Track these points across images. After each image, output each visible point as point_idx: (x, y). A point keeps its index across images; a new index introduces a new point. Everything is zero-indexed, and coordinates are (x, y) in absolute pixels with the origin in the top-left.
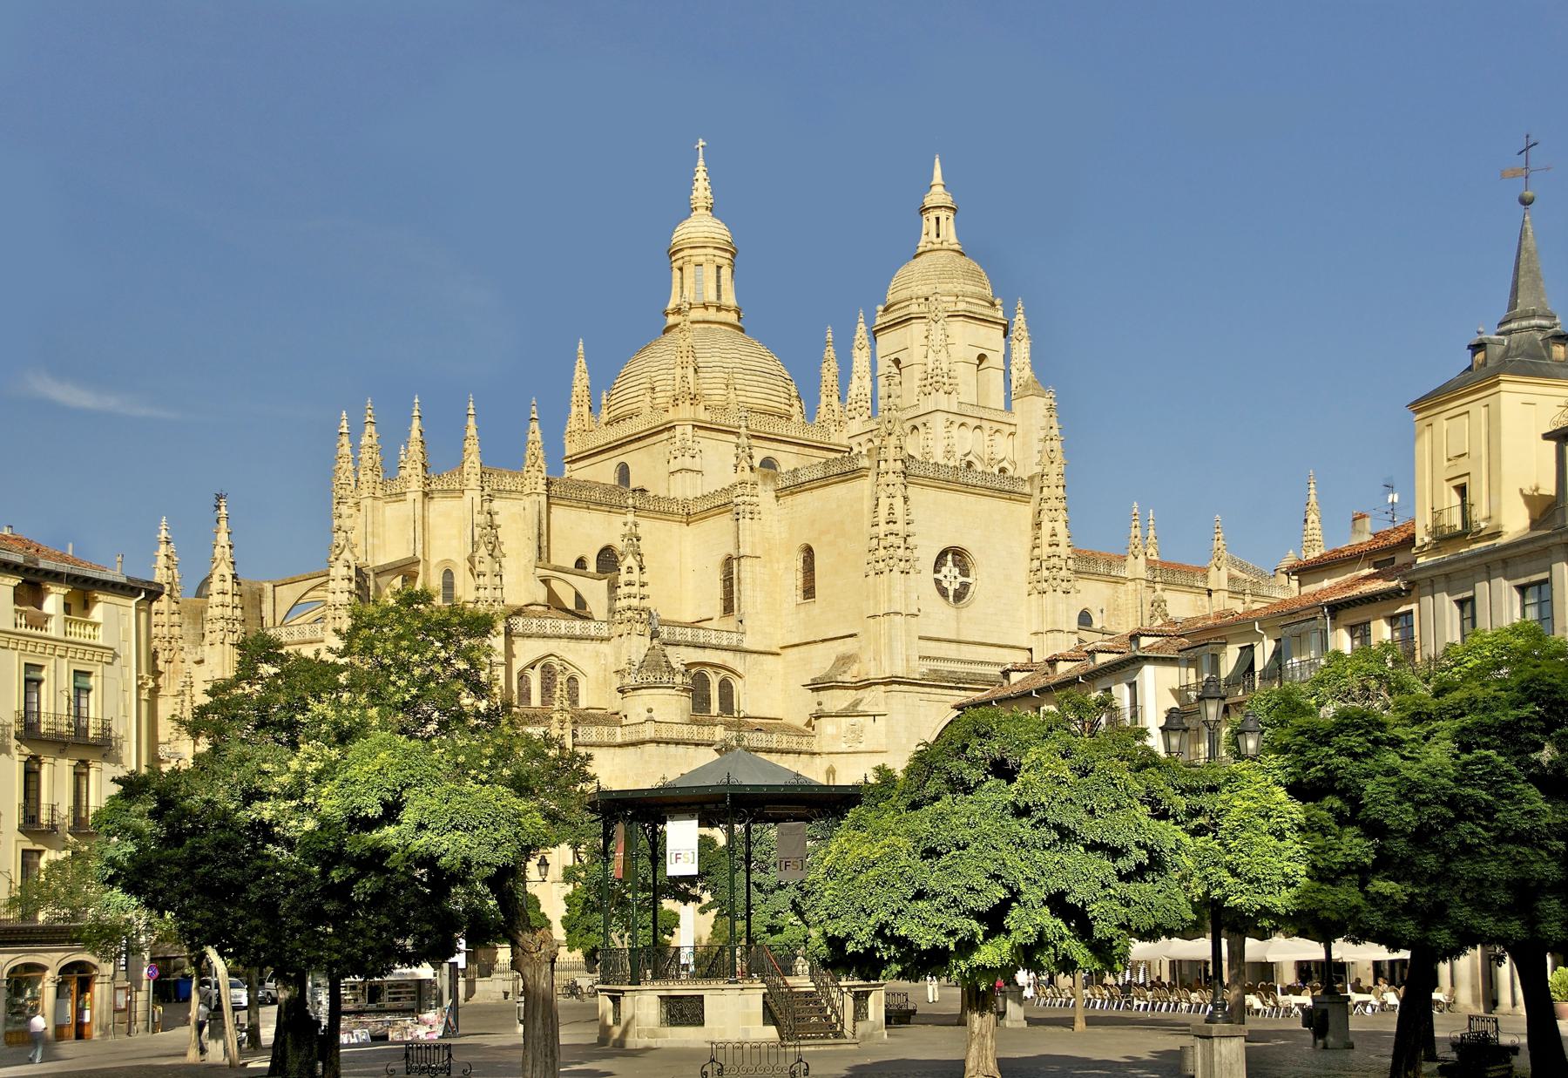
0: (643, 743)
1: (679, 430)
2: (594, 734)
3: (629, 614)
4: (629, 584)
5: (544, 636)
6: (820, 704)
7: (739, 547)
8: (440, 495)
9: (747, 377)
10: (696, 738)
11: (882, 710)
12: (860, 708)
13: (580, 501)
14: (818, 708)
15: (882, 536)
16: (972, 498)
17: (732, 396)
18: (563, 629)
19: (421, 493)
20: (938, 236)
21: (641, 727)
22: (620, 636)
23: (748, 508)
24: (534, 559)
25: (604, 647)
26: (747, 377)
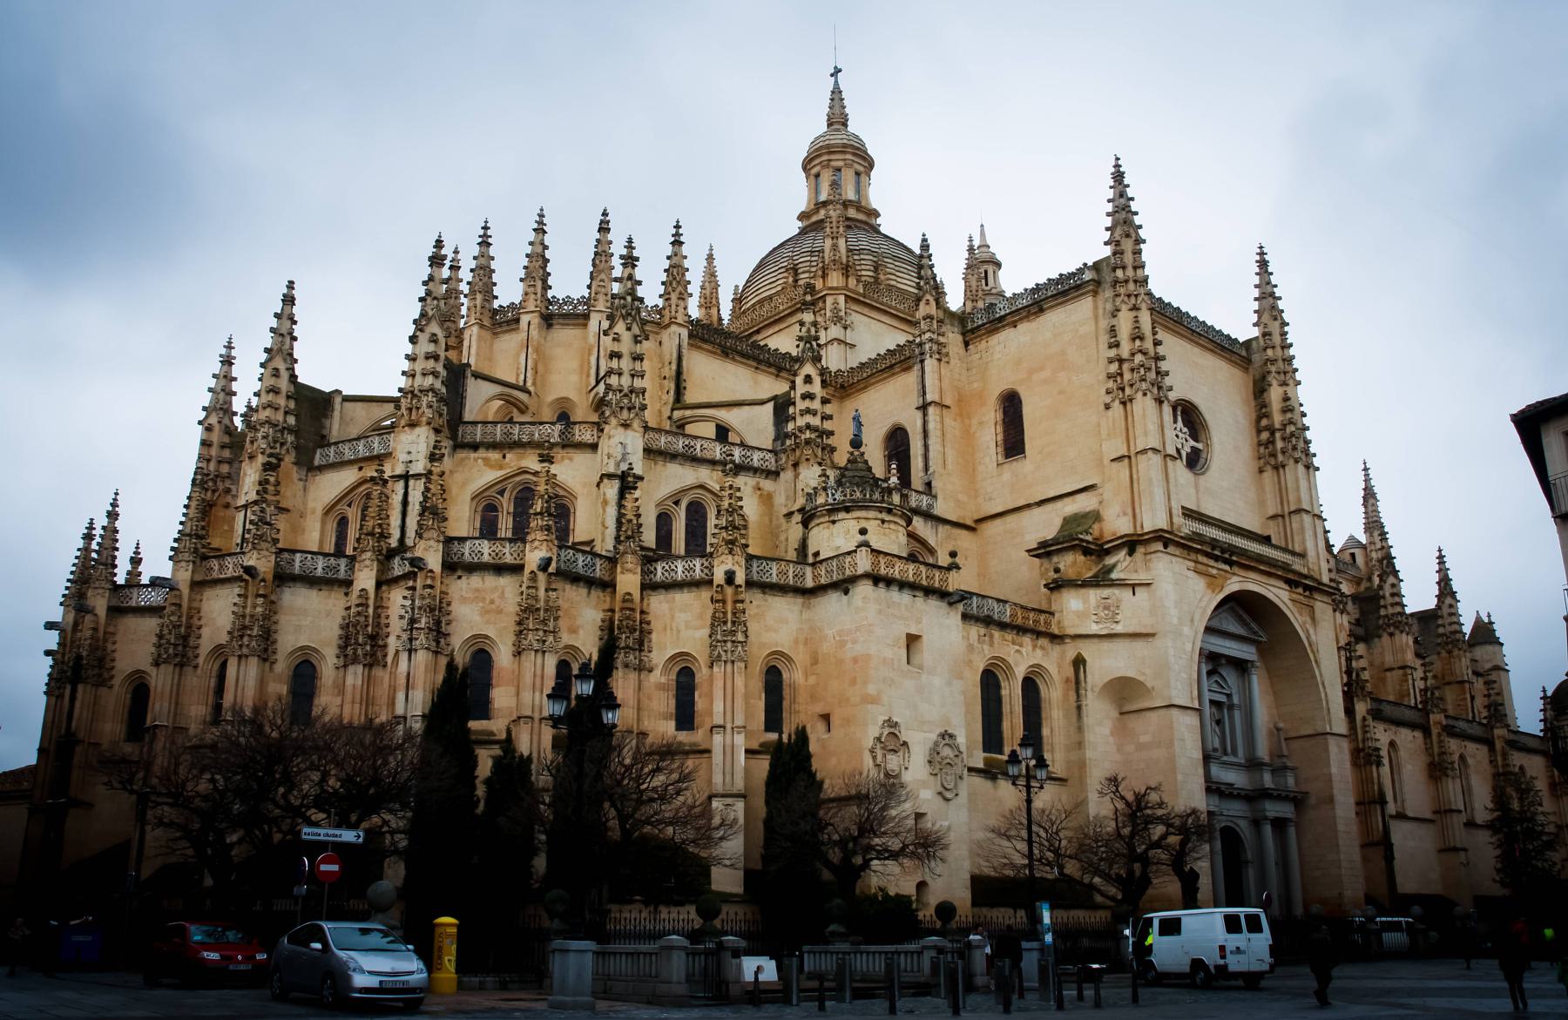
0: (854, 579)
1: (829, 300)
2: (774, 572)
3: (808, 435)
4: (808, 396)
6: (1057, 570)
7: (924, 393)
8: (561, 321)
9: (897, 263)
11: (1142, 576)
12: (1114, 576)
14: (1052, 575)
15: (1125, 354)
16: (1196, 350)
17: (882, 277)
20: (987, 285)
21: (848, 559)
22: (796, 465)
23: (935, 347)
25: (767, 485)
26: (897, 263)
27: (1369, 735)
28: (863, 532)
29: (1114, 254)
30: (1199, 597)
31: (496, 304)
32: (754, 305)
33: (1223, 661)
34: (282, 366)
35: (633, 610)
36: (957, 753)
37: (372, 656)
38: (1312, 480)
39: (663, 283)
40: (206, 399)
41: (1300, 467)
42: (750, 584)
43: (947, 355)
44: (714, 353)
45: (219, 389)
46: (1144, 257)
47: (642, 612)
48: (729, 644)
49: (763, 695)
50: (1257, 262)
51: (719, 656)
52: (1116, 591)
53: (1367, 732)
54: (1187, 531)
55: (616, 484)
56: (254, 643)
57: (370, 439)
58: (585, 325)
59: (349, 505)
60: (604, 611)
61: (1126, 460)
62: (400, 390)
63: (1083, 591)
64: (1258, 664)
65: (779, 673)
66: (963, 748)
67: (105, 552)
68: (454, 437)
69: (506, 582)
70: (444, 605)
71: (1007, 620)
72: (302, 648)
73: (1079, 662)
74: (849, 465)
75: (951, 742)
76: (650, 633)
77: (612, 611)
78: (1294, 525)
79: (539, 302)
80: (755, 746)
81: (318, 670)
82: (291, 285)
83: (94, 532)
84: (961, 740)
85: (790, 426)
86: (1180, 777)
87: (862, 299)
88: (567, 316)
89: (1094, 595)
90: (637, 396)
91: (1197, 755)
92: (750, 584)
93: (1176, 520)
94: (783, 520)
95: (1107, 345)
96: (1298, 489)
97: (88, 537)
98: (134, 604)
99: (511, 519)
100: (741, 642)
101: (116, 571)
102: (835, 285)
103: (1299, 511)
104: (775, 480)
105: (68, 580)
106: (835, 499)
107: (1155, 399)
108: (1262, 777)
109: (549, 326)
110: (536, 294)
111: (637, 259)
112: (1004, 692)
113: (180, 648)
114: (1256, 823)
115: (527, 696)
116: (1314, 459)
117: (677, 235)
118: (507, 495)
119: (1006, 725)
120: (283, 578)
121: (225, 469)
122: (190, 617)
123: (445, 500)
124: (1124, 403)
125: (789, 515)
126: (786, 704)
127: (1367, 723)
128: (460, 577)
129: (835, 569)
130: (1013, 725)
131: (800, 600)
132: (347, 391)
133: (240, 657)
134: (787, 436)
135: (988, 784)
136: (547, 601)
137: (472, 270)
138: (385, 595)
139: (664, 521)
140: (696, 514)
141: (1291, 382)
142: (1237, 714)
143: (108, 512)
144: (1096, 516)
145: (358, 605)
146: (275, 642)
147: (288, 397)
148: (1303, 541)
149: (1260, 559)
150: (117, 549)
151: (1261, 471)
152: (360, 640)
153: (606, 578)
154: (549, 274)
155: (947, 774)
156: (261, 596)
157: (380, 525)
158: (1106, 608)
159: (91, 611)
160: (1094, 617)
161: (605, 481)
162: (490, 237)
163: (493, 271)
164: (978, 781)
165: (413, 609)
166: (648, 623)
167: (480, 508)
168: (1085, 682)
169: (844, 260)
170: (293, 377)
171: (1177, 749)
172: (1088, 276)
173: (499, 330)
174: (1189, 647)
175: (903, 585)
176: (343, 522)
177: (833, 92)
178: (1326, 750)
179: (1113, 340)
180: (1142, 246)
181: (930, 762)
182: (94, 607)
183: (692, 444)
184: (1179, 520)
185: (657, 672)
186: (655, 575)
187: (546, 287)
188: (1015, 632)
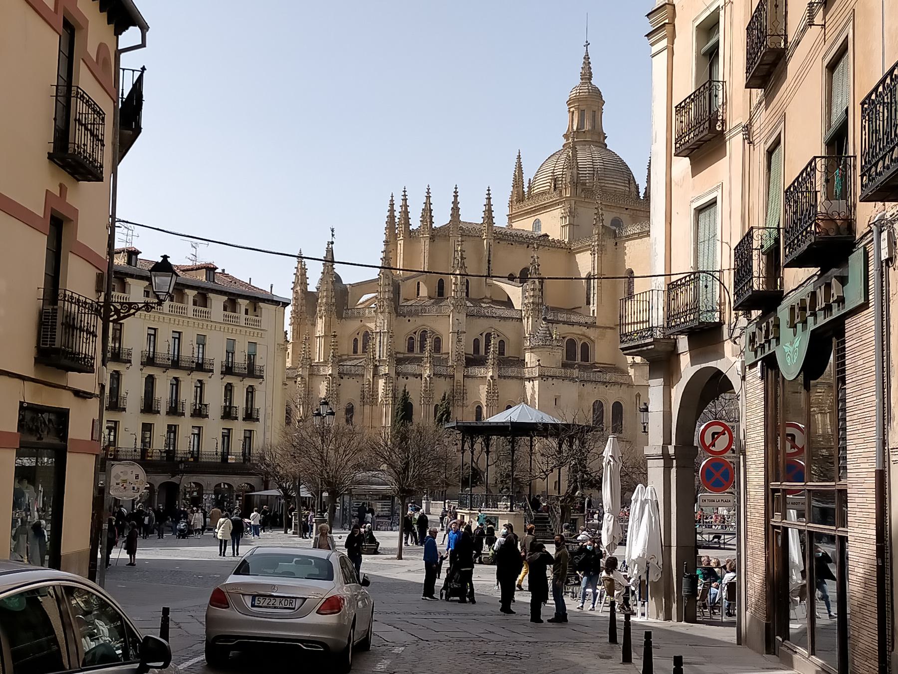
6: (633, 358)
22: (528, 318)
31: (411, 228)
39: (483, 218)
40: (293, 278)
59: (358, 334)
68: (397, 313)
73: (638, 395)
109: (434, 241)
117: (489, 194)
118: (417, 333)
120: (341, 375)
131: (519, 381)
139: (476, 342)
140: (488, 336)
167: (407, 339)
169: (575, 181)
175: (553, 377)
176: (356, 340)
177: (584, 58)
185: (469, 407)
187: (432, 223)
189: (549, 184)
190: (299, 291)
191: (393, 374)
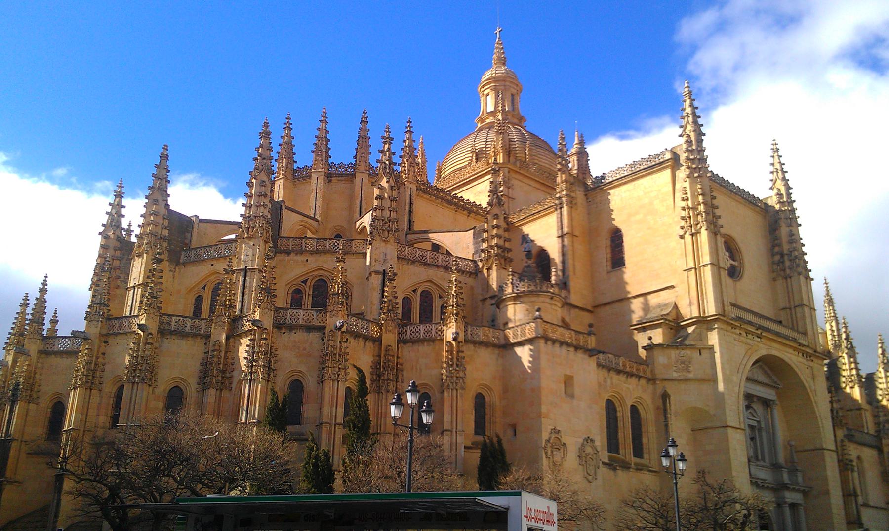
5: (426, 264)
6: (650, 338)
7: (562, 228)
10: (574, 343)
13: (437, 197)
14: (649, 342)
18: (440, 261)
19: (323, 173)
24: (406, 228)
26: (539, 150)
27: (845, 451)
28: (539, 310)
29: (687, 141)
30: (742, 357)
32: (450, 174)
33: (755, 400)
34: (160, 199)
35: (393, 356)
36: (596, 452)
37: (222, 383)
38: (809, 287)
40: (105, 219)
41: (802, 278)
42: (466, 341)
43: (576, 204)
44: (432, 200)
45: (114, 212)
46: (704, 144)
47: (398, 357)
48: (455, 378)
49: (474, 411)
50: (772, 149)
51: (448, 385)
52: (688, 352)
53: (844, 449)
54: (733, 316)
55: (381, 277)
56: (143, 375)
57: (218, 247)
58: (352, 181)
59: (204, 288)
60: (373, 356)
61: (693, 271)
62: (242, 215)
63: (667, 351)
64: (777, 402)
65: (483, 398)
66: (599, 449)
67: (37, 314)
68: (275, 246)
69: (314, 336)
70: (273, 351)
71: (621, 368)
72: (174, 378)
73: (665, 396)
74: (526, 269)
75: (591, 444)
76: (402, 371)
77: (380, 356)
78: (798, 315)
79: (324, 166)
80: (469, 444)
81: (185, 393)
82: (166, 148)
83: (28, 302)
84: (598, 443)
85: (484, 246)
86: (734, 474)
87: (518, 171)
88: (341, 175)
89: (674, 354)
90: (393, 222)
91: (747, 461)
92: (466, 341)
93: (726, 308)
94: (480, 303)
95: (680, 199)
96: (800, 291)
97: (24, 305)
98: (56, 350)
99: (310, 298)
100: (462, 377)
101: (44, 327)
102: (501, 162)
103: (802, 305)
104: (475, 278)
105: (10, 333)
106: (518, 290)
107: (712, 233)
108: (782, 477)
109: (330, 181)
110: (322, 160)
111: (392, 139)
112: (619, 414)
113: (90, 378)
114: (779, 505)
115: (326, 410)
116: (810, 273)
118: (308, 283)
119: (620, 435)
120: (163, 332)
121: (116, 263)
122: (97, 358)
123: (275, 284)
124: (692, 235)
125: (484, 300)
126: (487, 417)
127: (844, 443)
128: (284, 333)
129: (519, 333)
130: (625, 434)
131: (496, 351)
132: (202, 216)
133: (133, 384)
134: (483, 251)
135: (612, 473)
136: (341, 349)
137: (280, 145)
138: (231, 344)
139: (407, 301)
140: (426, 297)
141: (794, 224)
142: (764, 434)
143: (40, 288)
144: (676, 307)
145: (213, 351)
146: (155, 374)
147: (164, 218)
148: (805, 324)
149: (778, 334)
150: (45, 313)
151: (774, 280)
152: (215, 375)
153: (376, 335)
154: (330, 149)
155: (590, 465)
156: (149, 344)
157: (230, 300)
158: (683, 362)
159: (27, 354)
160: (675, 368)
161: (373, 275)
162: (292, 124)
163: (294, 146)
164: (603, 471)
165: (253, 353)
166: (401, 365)
167: (291, 291)
168: (670, 409)
169: (508, 146)
170: (167, 206)
171: (732, 456)
172: (668, 156)
173: (297, 182)
174: (736, 389)
175: (562, 343)
176: (199, 299)
178: (824, 460)
179: (684, 196)
180: (703, 137)
181: (579, 457)
182: (29, 351)
183: (425, 255)
184: (728, 308)
186: (406, 335)
188: (625, 376)
189: (470, 158)
190: (112, 236)
191: (268, 323)
